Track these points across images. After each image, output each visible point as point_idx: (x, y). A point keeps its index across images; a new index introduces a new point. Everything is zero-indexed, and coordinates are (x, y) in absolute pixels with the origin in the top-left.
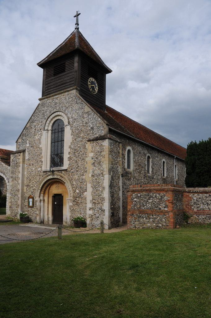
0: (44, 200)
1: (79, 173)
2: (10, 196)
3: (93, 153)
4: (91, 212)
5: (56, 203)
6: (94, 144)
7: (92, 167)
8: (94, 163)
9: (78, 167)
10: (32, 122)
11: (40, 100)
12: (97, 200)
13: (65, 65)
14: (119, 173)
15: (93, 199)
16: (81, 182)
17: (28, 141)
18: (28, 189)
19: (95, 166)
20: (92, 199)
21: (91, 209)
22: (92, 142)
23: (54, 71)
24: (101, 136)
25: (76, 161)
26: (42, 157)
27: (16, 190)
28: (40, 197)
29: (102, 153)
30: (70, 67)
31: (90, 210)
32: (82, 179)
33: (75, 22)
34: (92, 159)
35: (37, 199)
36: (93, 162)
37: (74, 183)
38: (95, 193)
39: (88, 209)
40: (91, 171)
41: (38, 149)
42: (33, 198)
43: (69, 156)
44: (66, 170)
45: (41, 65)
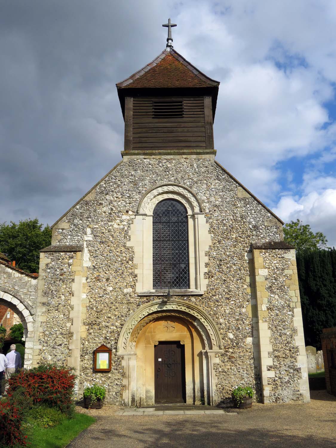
1: (232, 302)
2: (40, 347)
3: (266, 270)
4: (272, 374)
5: (160, 360)
6: (267, 254)
7: (268, 294)
8: (271, 287)
9: (230, 291)
10: (102, 193)
12: (282, 353)
15: (274, 350)
16: (238, 320)
17: (89, 231)
18: (91, 331)
19: (272, 292)
20: (272, 351)
21: (271, 367)
22: (263, 251)
23: (155, 109)
24: (275, 243)
25: (225, 280)
26: (134, 267)
27: (62, 334)
29: (286, 272)
30: (195, 113)
31: (269, 370)
32: (240, 314)
34: (266, 279)
36: (269, 285)
37: (221, 321)
38: (276, 339)
40: (266, 300)
41: (123, 248)
43: (206, 270)
44: (201, 295)
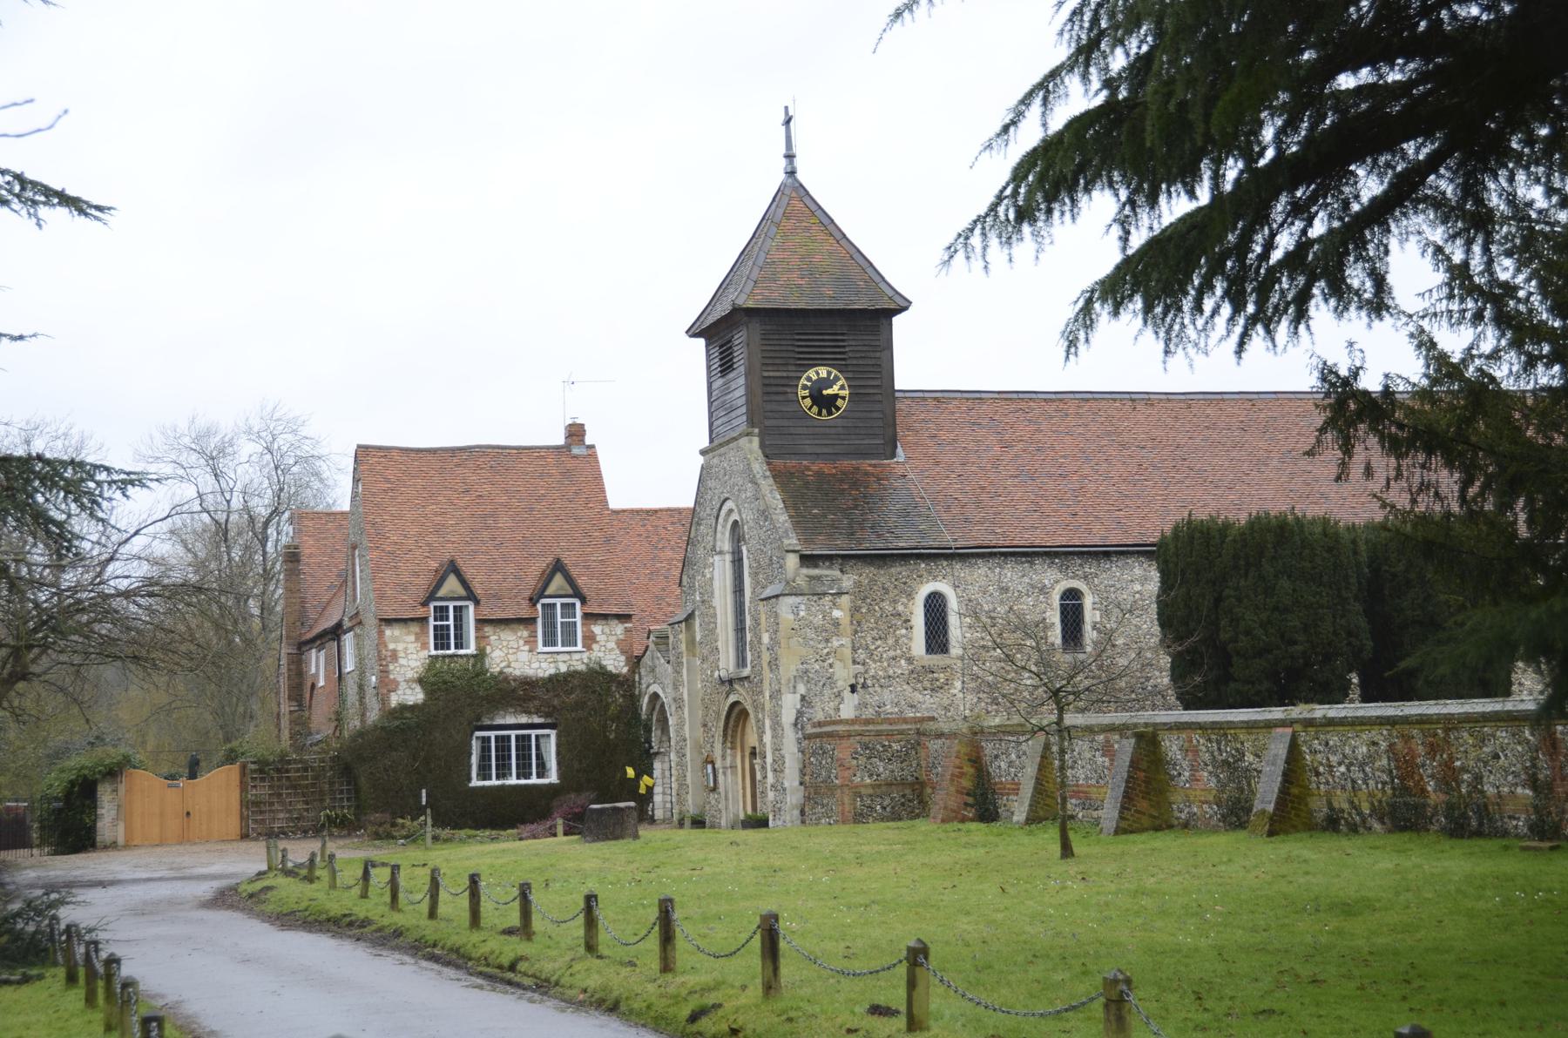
0: (733, 767)
11: (703, 452)
13: (731, 347)
14: (840, 683)
28: (724, 757)
33: (783, 151)
35: (718, 765)
39: (769, 788)
42: (713, 763)
45: (693, 332)
